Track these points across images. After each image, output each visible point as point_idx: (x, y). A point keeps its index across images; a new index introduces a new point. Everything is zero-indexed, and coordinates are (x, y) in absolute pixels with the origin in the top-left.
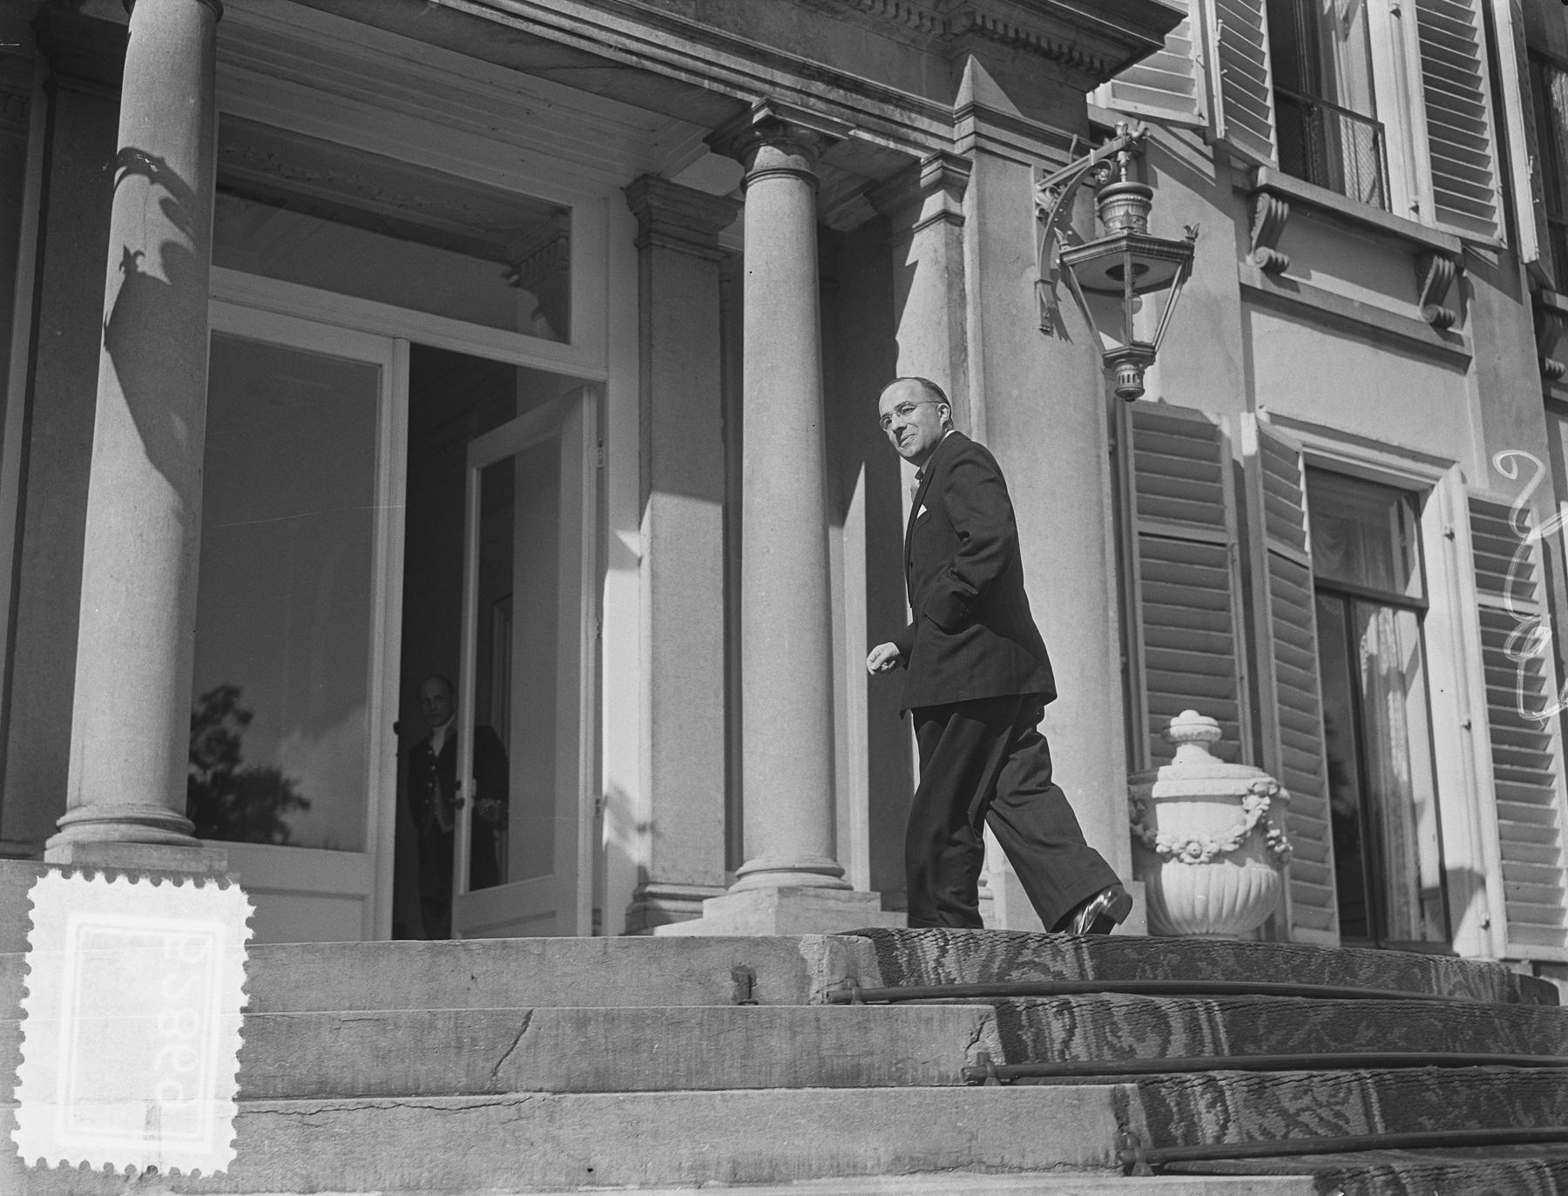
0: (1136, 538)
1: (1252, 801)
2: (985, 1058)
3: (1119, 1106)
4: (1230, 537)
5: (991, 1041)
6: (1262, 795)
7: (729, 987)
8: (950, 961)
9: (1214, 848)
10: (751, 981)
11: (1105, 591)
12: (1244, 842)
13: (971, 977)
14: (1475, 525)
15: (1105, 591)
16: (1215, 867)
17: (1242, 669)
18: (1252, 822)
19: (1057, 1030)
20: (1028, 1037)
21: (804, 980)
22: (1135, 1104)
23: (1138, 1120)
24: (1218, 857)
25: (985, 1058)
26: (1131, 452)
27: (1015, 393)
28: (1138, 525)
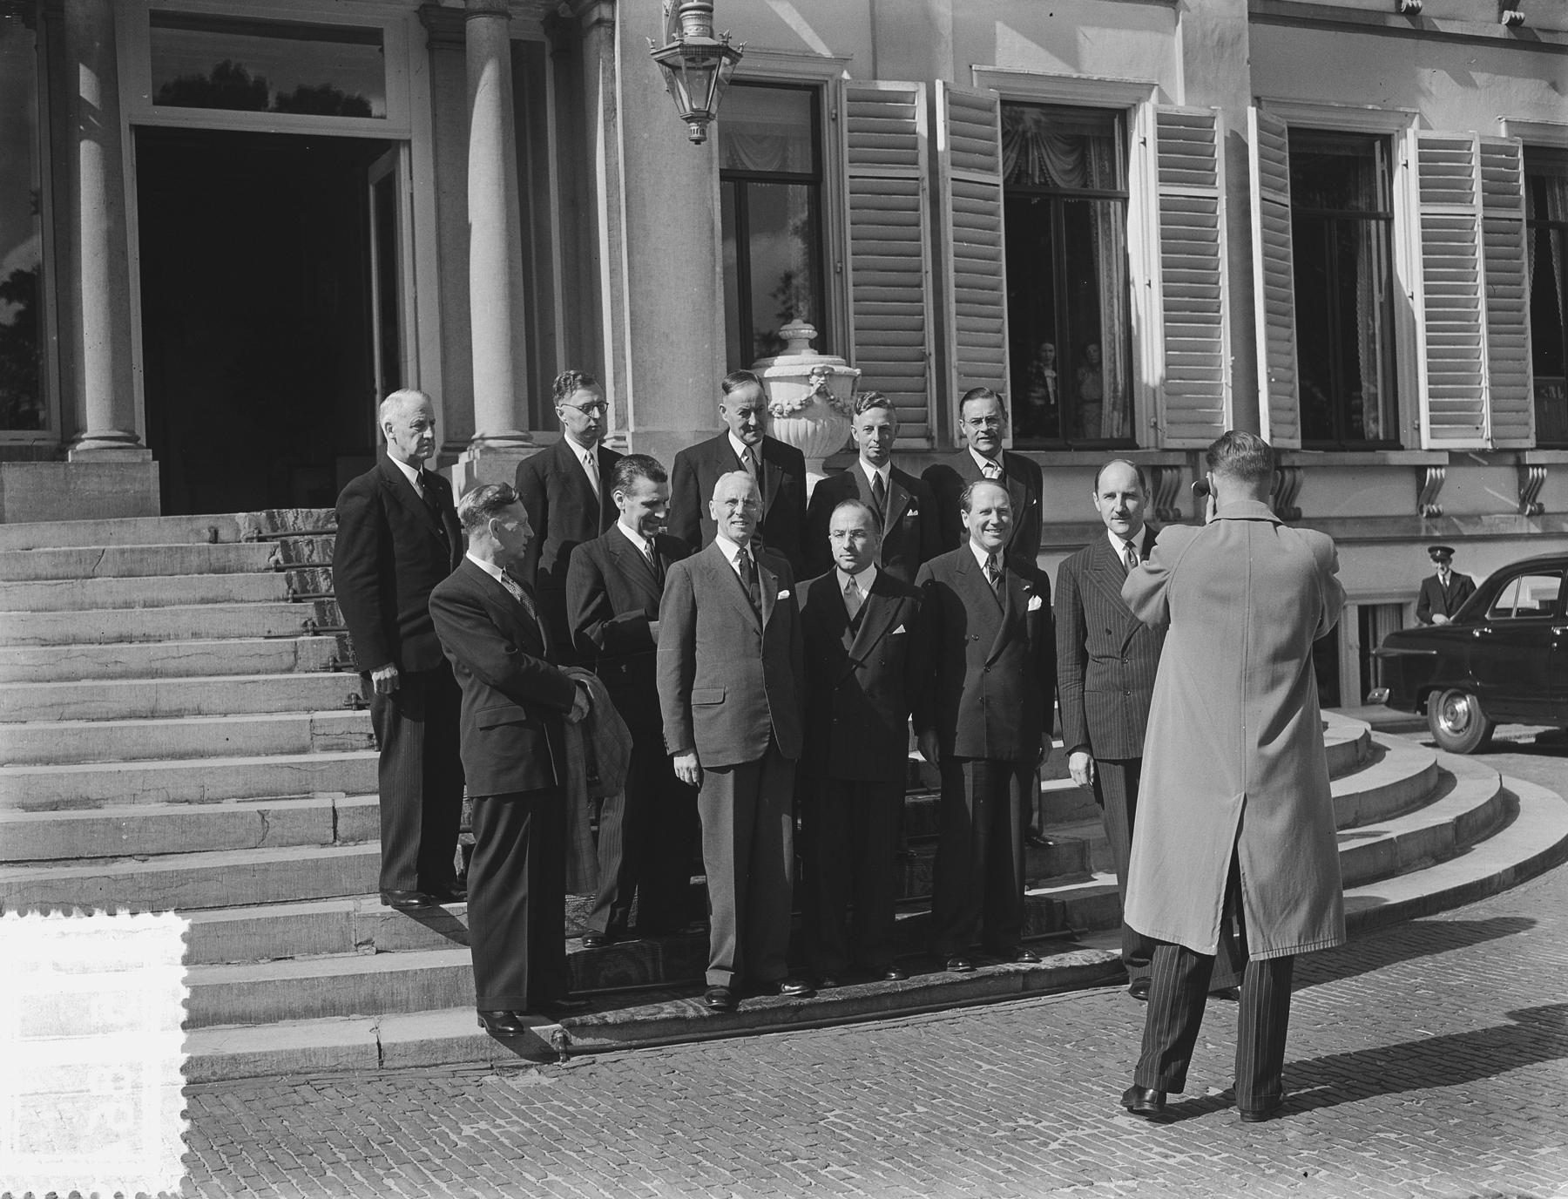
0: (847, 181)
1: (814, 378)
2: (277, 562)
3: (289, 580)
4: (923, 171)
5: (279, 555)
6: (820, 375)
7: (208, 535)
8: (299, 521)
9: (788, 408)
10: (216, 533)
11: (713, 255)
12: (807, 403)
13: (309, 528)
14: (1161, 135)
15: (713, 255)
16: (792, 420)
17: (928, 265)
18: (813, 390)
19: (306, 551)
20: (293, 554)
21: (238, 531)
22: (295, 579)
23: (295, 585)
24: (793, 413)
25: (277, 562)
26: (846, 119)
27: (646, 135)
28: (849, 170)
